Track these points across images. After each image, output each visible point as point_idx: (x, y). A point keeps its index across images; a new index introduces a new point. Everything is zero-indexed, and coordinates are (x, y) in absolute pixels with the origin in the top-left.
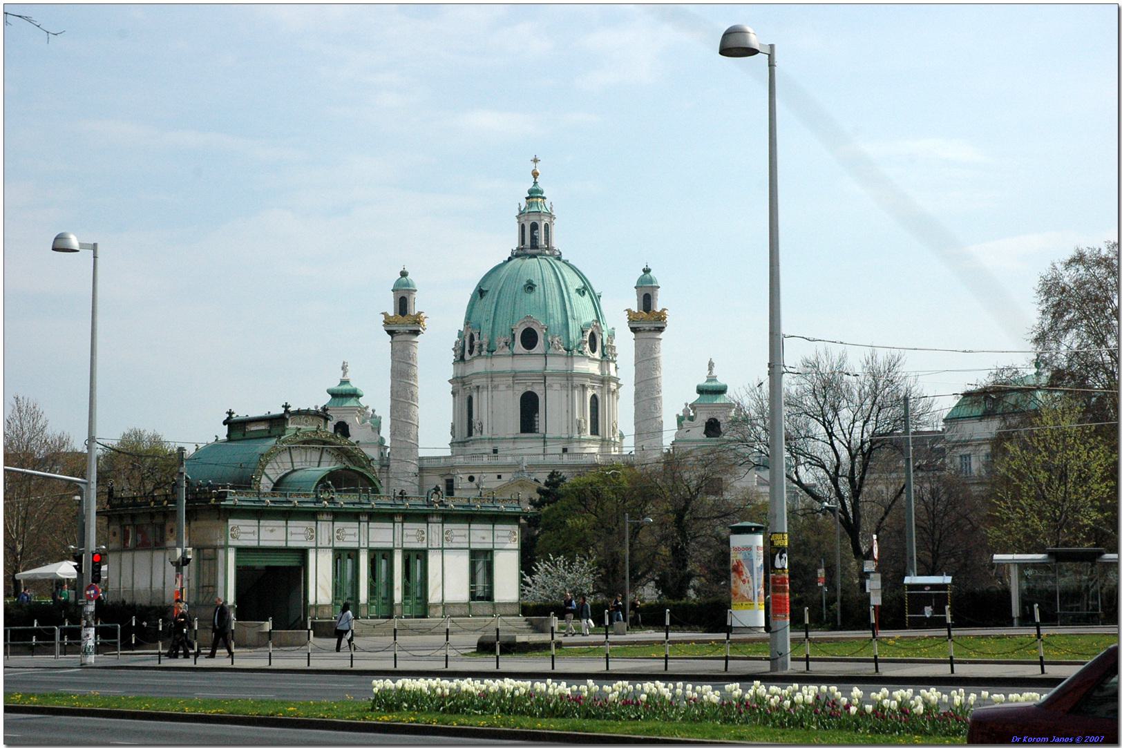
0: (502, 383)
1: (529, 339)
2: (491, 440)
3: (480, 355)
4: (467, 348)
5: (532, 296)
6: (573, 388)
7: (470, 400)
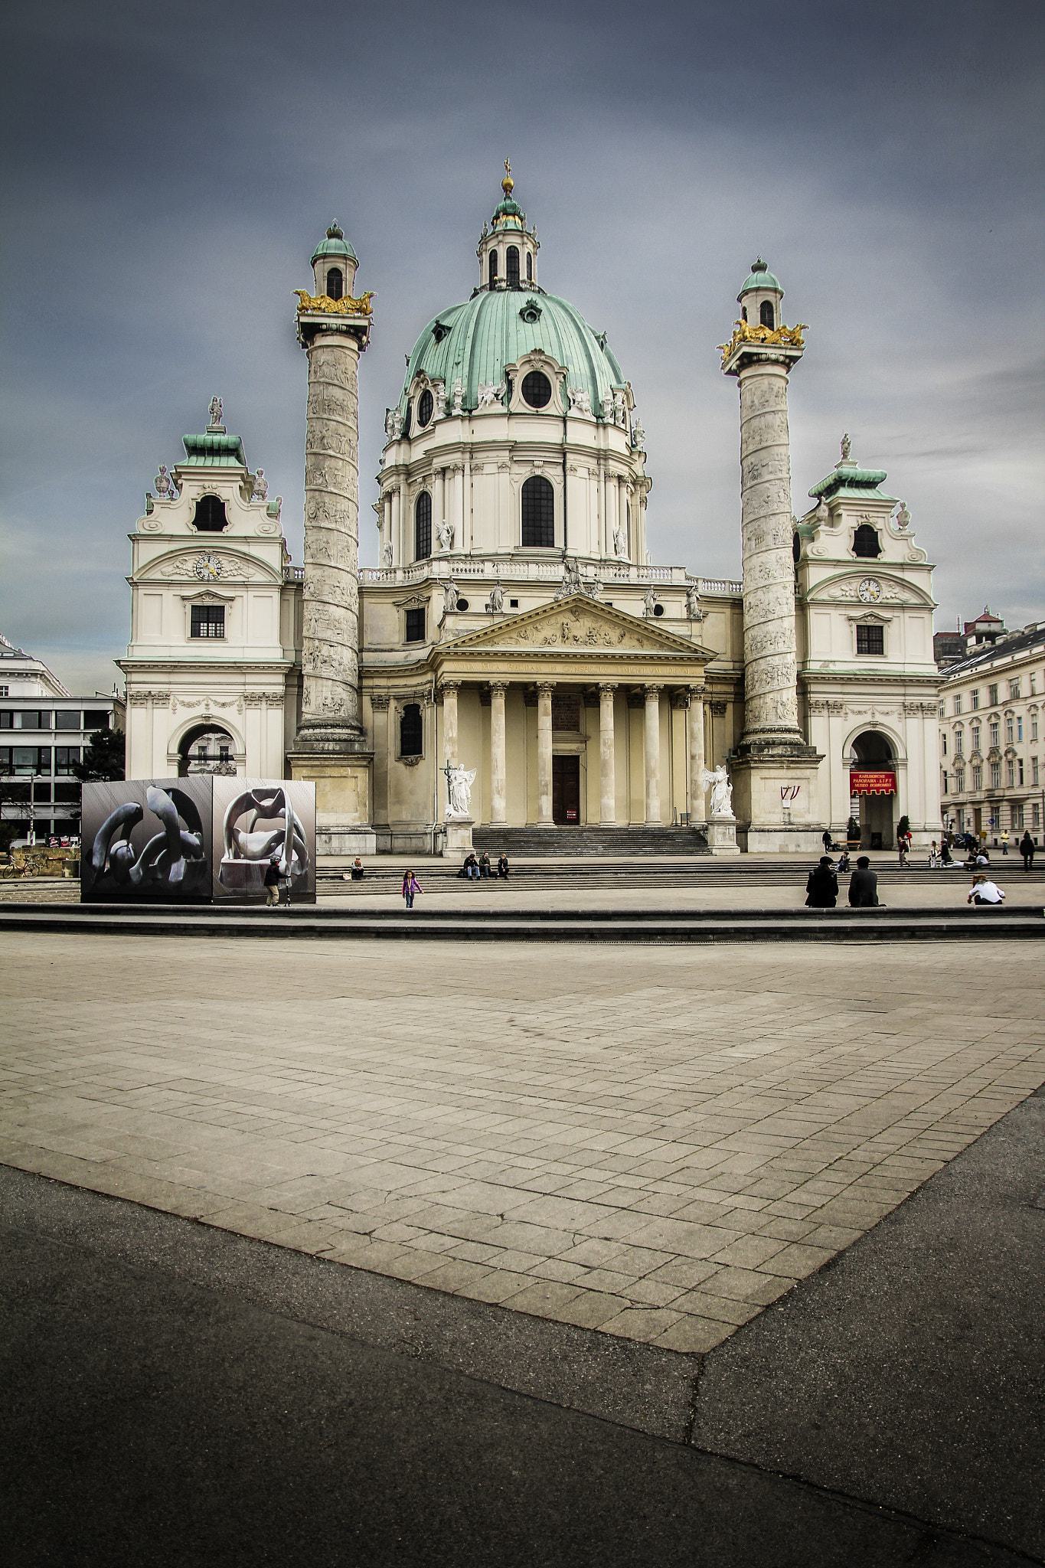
0: (490, 460)
1: (537, 390)
3: (449, 415)
5: (536, 326)
6: (607, 476)
7: (423, 504)
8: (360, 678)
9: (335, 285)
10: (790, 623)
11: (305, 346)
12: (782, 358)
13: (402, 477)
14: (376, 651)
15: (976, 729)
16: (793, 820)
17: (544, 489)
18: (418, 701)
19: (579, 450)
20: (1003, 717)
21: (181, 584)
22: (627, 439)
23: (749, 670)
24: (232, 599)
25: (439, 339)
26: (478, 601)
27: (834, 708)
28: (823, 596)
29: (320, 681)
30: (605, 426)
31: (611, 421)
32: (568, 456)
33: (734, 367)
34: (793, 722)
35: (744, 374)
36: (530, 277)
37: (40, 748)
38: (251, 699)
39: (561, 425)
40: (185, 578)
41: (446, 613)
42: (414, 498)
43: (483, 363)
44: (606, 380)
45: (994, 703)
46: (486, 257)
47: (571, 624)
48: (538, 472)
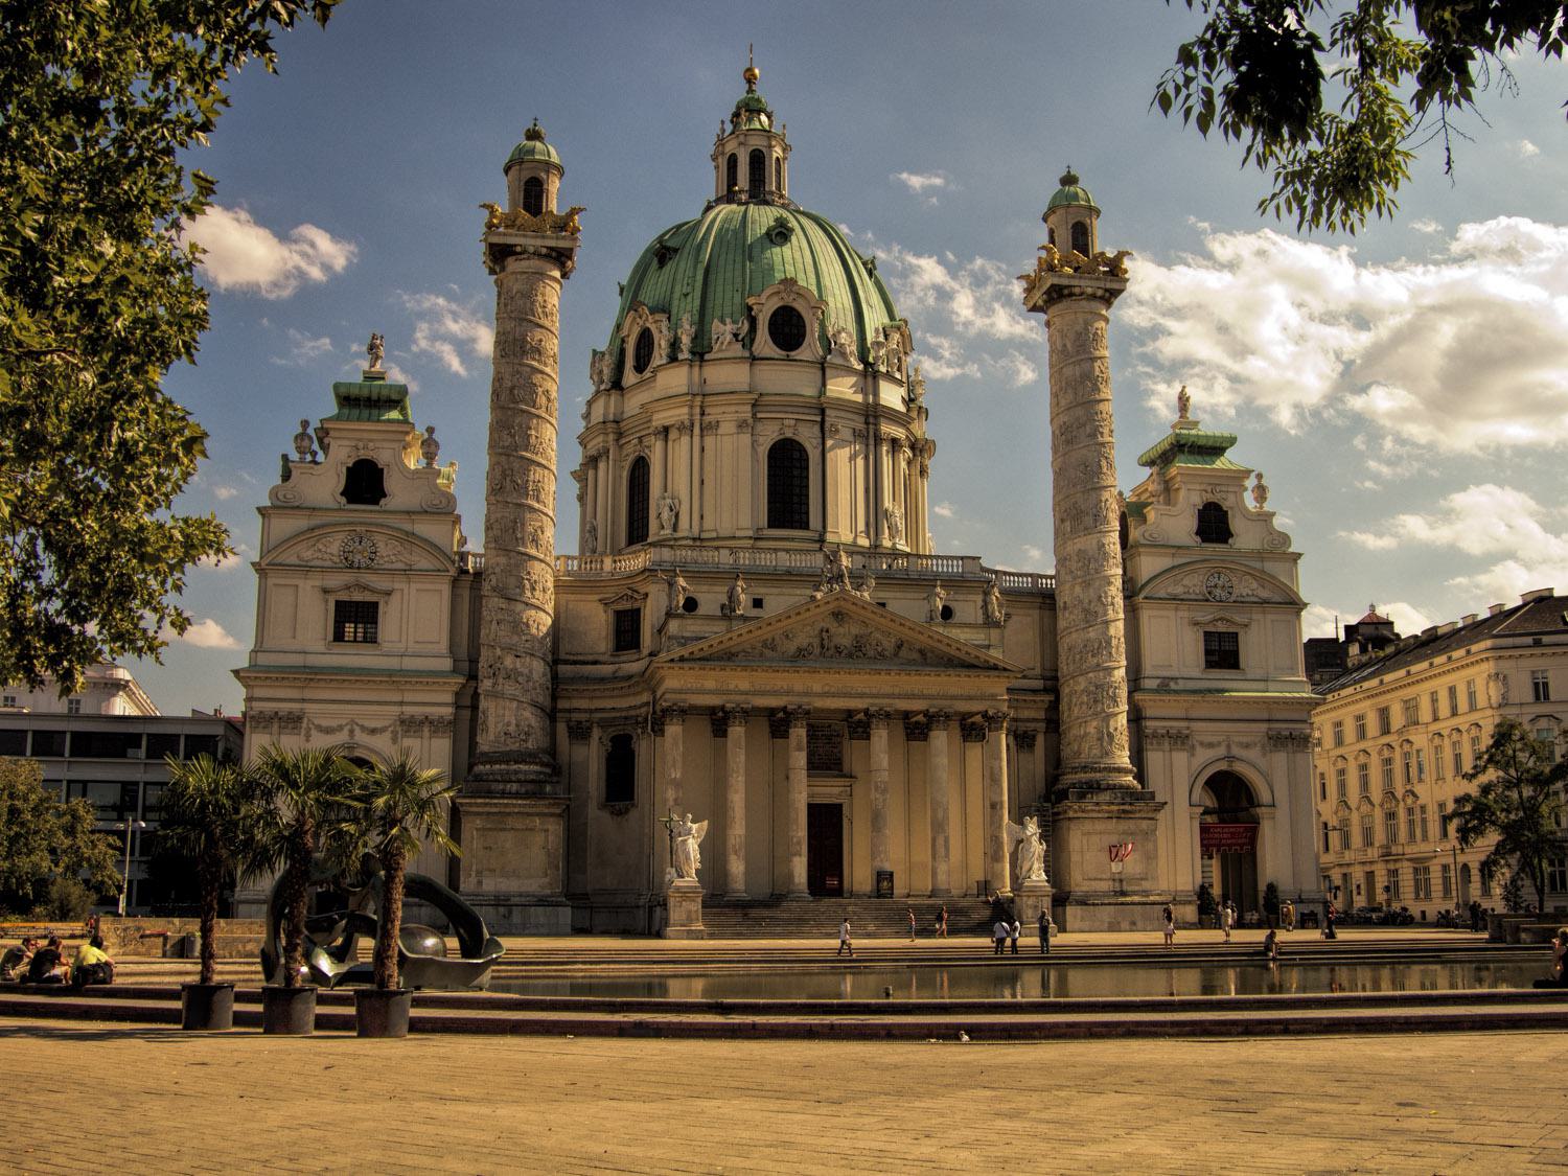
0: (727, 416)
1: (789, 328)
2: (698, 541)
3: (673, 359)
4: (630, 362)
5: (786, 249)
6: (878, 440)
7: (640, 469)
8: (554, 698)
9: (532, 194)
10: (1118, 629)
11: (492, 272)
12: (1100, 293)
13: (611, 437)
14: (575, 663)
15: (1364, 767)
16: (1125, 888)
17: (796, 455)
18: (629, 730)
19: (843, 405)
20: (1398, 749)
21: (323, 570)
22: (902, 391)
23: (1065, 691)
24: (389, 593)
25: (662, 263)
26: (711, 599)
27: (1180, 740)
28: (1162, 594)
29: (501, 702)
30: (876, 375)
31: (883, 369)
32: (828, 412)
33: (1040, 303)
34: (1123, 758)
35: (1054, 310)
36: (779, 187)
37: (124, 784)
38: (410, 725)
39: (819, 373)
40: (328, 564)
41: (669, 615)
42: (627, 465)
43: (719, 294)
44: (875, 318)
45: (1386, 730)
46: (723, 162)
47: (832, 630)
48: (789, 434)
